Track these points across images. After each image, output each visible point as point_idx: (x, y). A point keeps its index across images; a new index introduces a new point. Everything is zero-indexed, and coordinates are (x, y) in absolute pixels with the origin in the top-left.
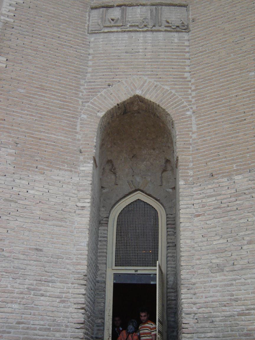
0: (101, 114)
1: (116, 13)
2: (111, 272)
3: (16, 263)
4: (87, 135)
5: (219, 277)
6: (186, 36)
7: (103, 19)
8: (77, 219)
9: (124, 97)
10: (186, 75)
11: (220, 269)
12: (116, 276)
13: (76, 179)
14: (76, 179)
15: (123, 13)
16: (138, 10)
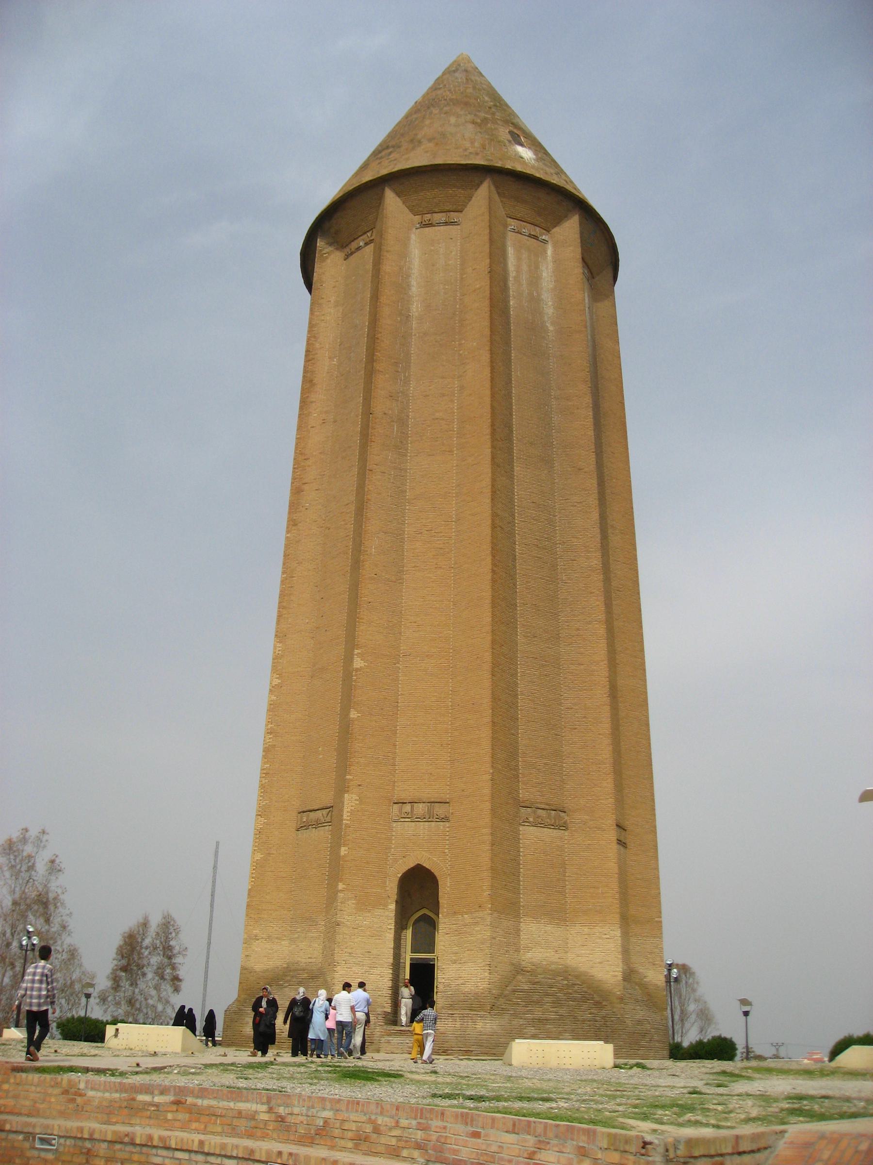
0: (399, 875)
1: (407, 808)
2: (408, 957)
3: (359, 959)
4: (392, 888)
5: (454, 965)
6: (447, 824)
7: (400, 810)
8: (387, 934)
9: (412, 865)
10: (446, 851)
11: (455, 962)
12: (411, 959)
13: (387, 913)
14: (387, 913)
15: (412, 807)
16: (421, 805)
